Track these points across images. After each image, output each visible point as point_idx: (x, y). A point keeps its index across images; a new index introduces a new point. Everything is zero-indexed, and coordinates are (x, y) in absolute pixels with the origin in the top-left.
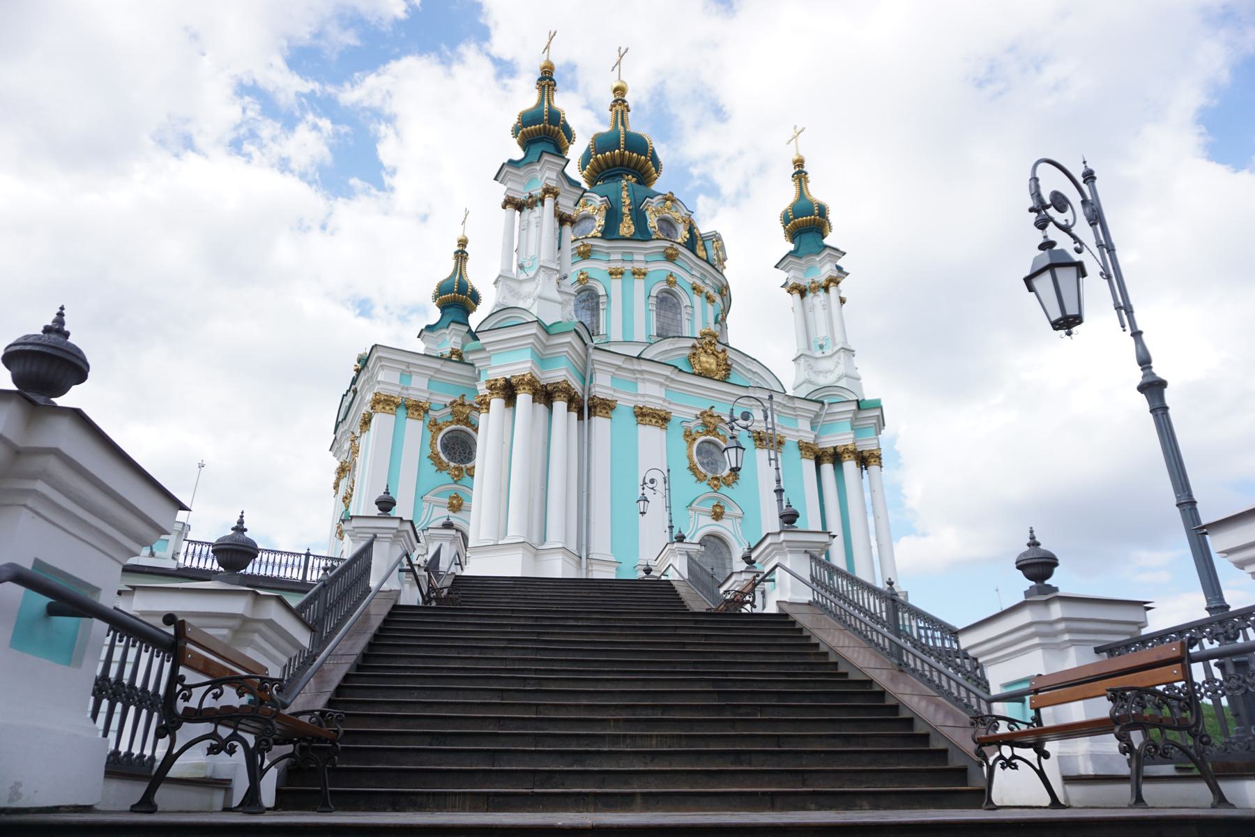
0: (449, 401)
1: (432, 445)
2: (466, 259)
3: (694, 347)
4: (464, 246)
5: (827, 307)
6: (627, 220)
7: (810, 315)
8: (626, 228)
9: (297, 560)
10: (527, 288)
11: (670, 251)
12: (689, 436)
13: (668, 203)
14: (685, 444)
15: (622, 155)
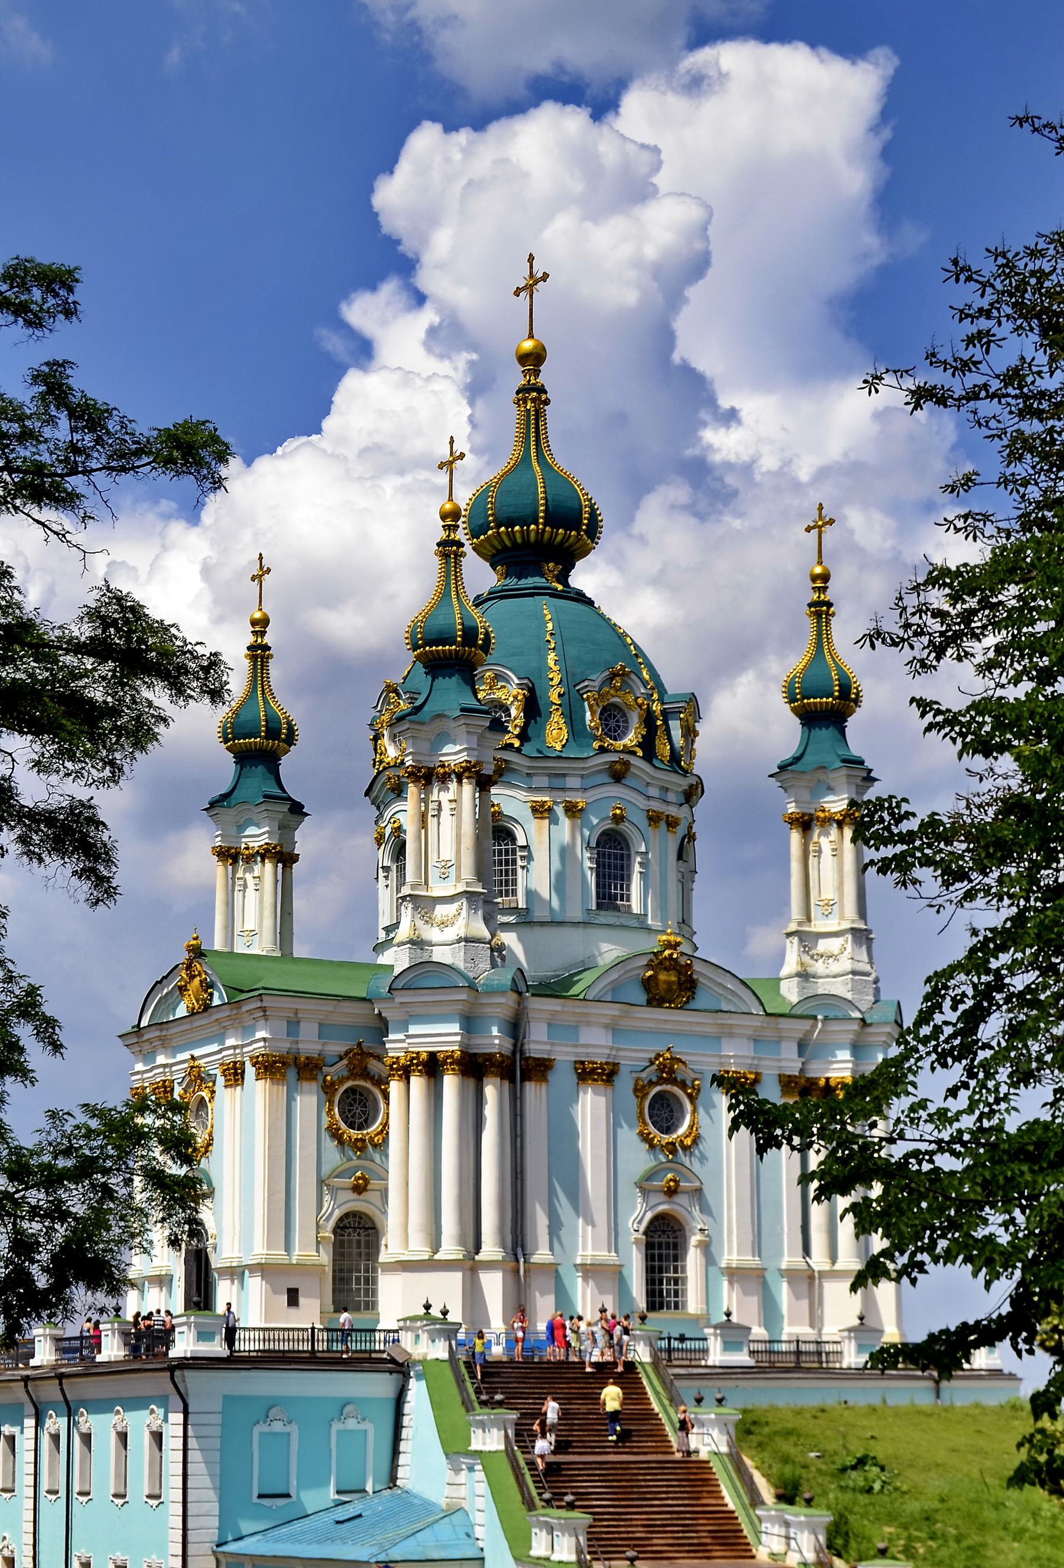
0: (344, 1049)
1: (330, 1110)
2: (270, 656)
3: (649, 966)
4: (263, 634)
5: (837, 853)
6: (556, 717)
7: (812, 861)
8: (555, 733)
9: (306, 1334)
10: (442, 911)
11: (618, 767)
12: (640, 1091)
13: (618, 678)
14: (633, 1101)
15: (540, 534)
